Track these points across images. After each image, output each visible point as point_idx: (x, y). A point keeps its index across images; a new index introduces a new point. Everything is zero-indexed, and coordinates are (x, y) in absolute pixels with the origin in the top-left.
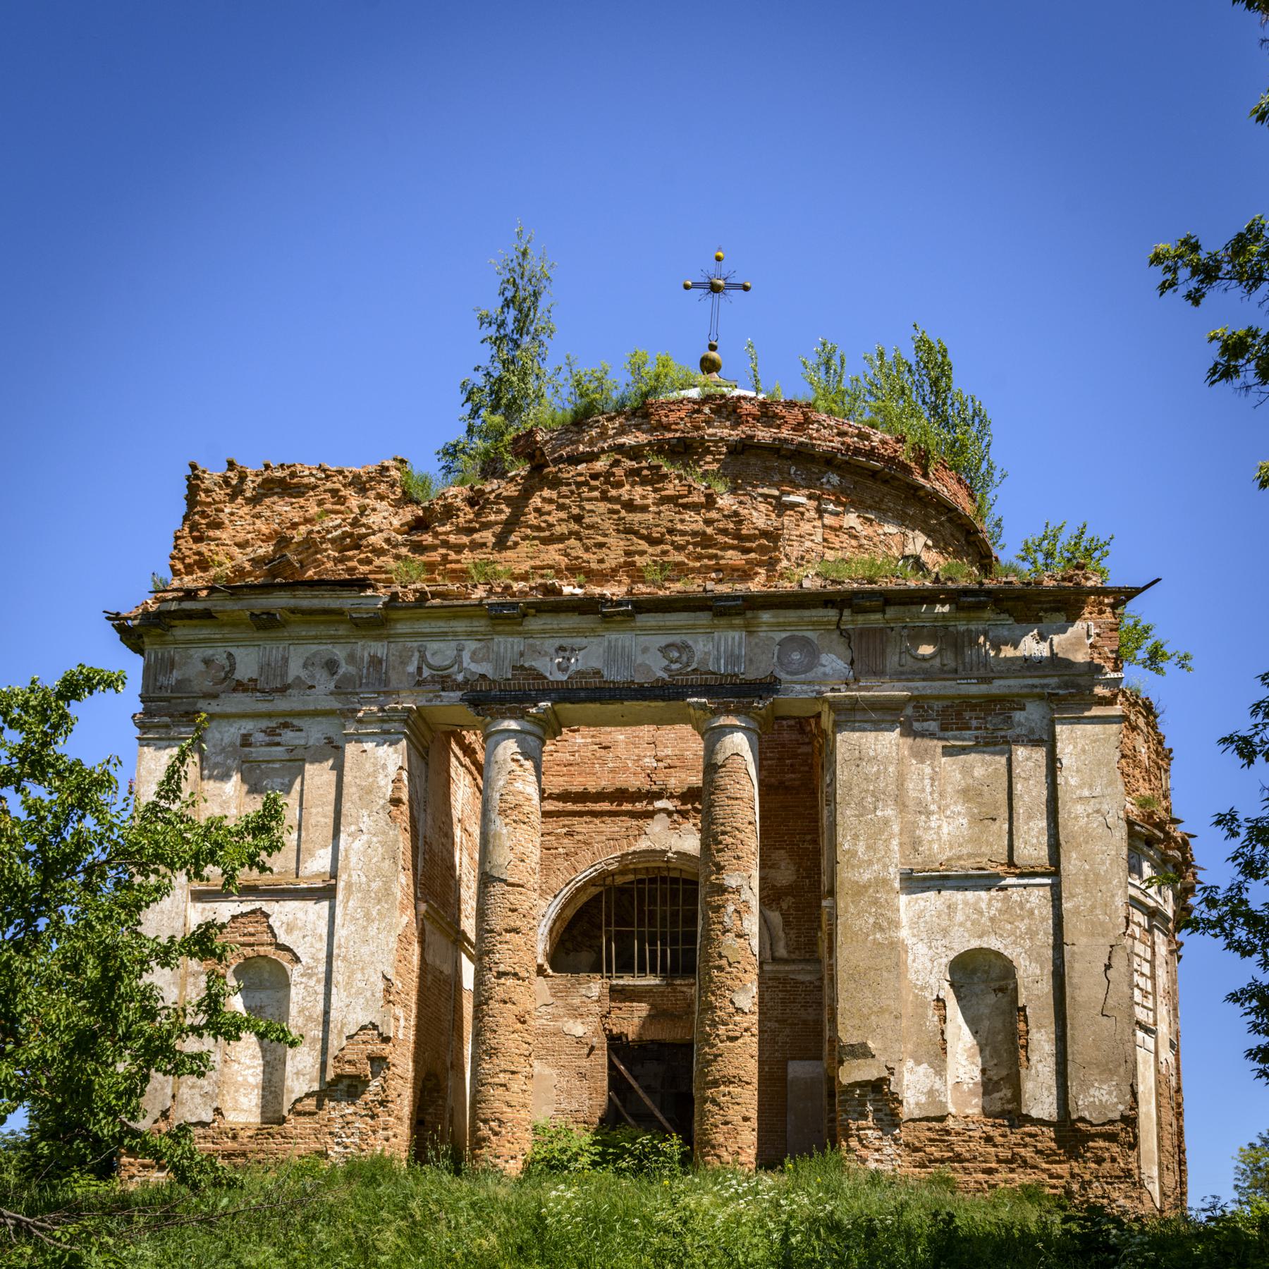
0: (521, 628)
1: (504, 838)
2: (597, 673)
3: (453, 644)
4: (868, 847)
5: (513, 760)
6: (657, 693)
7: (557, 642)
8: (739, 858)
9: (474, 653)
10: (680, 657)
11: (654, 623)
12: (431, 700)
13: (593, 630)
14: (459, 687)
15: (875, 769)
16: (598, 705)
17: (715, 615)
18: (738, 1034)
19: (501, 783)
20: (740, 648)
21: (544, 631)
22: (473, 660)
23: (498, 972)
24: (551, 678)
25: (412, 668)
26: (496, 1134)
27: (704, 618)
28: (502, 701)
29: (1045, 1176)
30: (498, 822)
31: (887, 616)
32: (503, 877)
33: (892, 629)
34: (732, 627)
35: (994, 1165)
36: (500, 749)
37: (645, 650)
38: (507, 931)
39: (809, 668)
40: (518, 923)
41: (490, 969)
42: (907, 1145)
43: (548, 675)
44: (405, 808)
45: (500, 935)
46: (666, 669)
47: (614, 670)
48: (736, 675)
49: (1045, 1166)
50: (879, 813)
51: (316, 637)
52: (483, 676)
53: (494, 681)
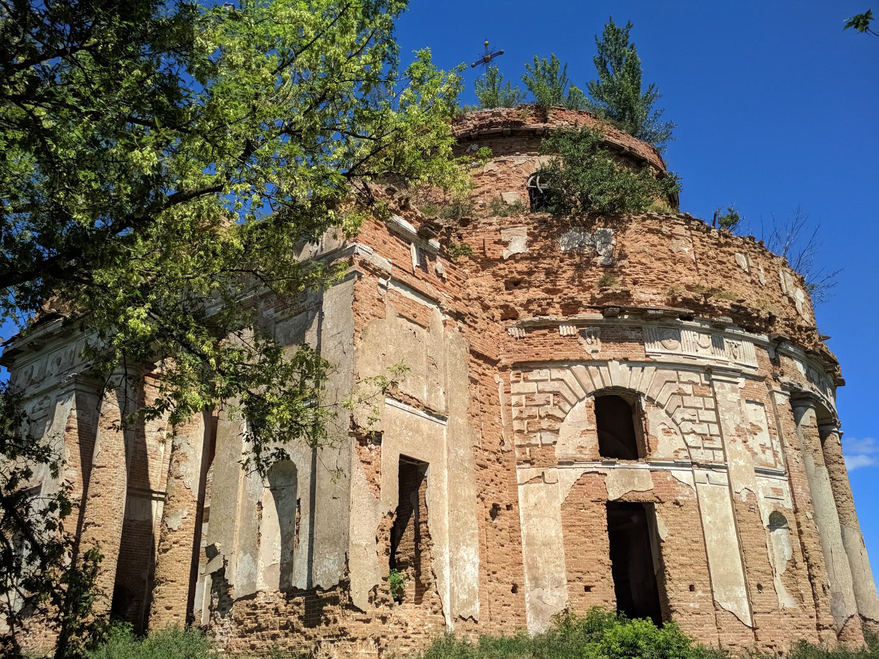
18: (168, 547)
29: (303, 638)
35: (277, 632)
40: (99, 490)
42: (236, 620)
44: (75, 432)
49: (303, 629)
51: (55, 348)
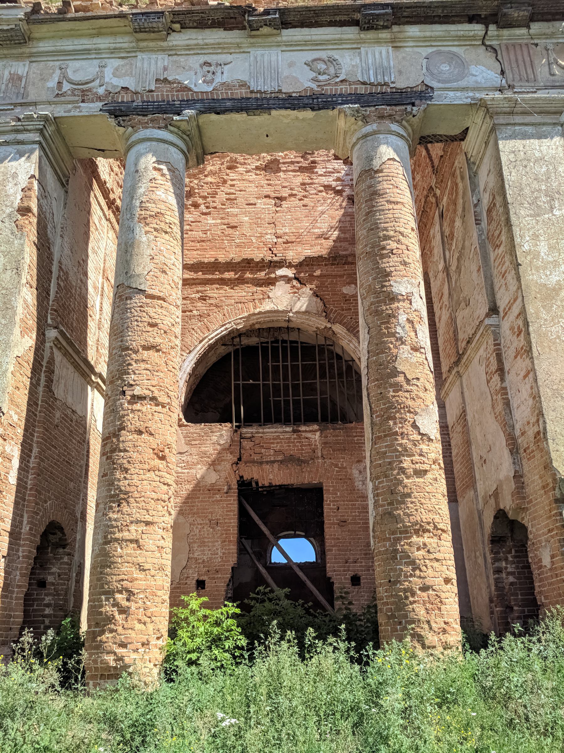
0: (164, 44)
1: (144, 246)
2: (243, 85)
3: (96, 62)
4: (551, 248)
5: (155, 169)
6: (306, 101)
7: (202, 59)
8: (405, 264)
9: (117, 69)
10: (327, 69)
11: (299, 38)
12: (69, 111)
13: (238, 46)
14: (100, 99)
15: (544, 169)
16: (245, 115)
17: (363, 29)
19: (142, 190)
20: (389, 62)
21: (188, 48)
22: (114, 75)
23: (133, 396)
24: (195, 89)
25: (52, 84)
26: (123, 611)
27: (351, 32)
28: (143, 111)
30: (137, 230)
31: (531, 31)
32: (142, 287)
33: (536, 45)
34: (378, 42)
36: (143, 160)
37: (291, 65)
38: (146, 348)
39: (462, 76)
40: (158, 340)
41: (124, 393)
43: (192, 86)
45: (136, 352)
46: (314, 80)
47: (261, 81)
48: (386, 84)
50: (557, 212)
52: (125, 89)
53: (136, 93)
